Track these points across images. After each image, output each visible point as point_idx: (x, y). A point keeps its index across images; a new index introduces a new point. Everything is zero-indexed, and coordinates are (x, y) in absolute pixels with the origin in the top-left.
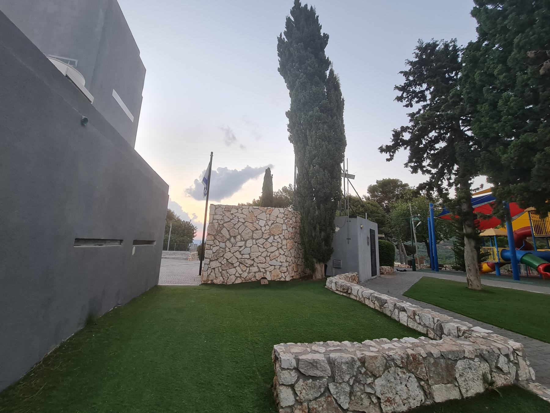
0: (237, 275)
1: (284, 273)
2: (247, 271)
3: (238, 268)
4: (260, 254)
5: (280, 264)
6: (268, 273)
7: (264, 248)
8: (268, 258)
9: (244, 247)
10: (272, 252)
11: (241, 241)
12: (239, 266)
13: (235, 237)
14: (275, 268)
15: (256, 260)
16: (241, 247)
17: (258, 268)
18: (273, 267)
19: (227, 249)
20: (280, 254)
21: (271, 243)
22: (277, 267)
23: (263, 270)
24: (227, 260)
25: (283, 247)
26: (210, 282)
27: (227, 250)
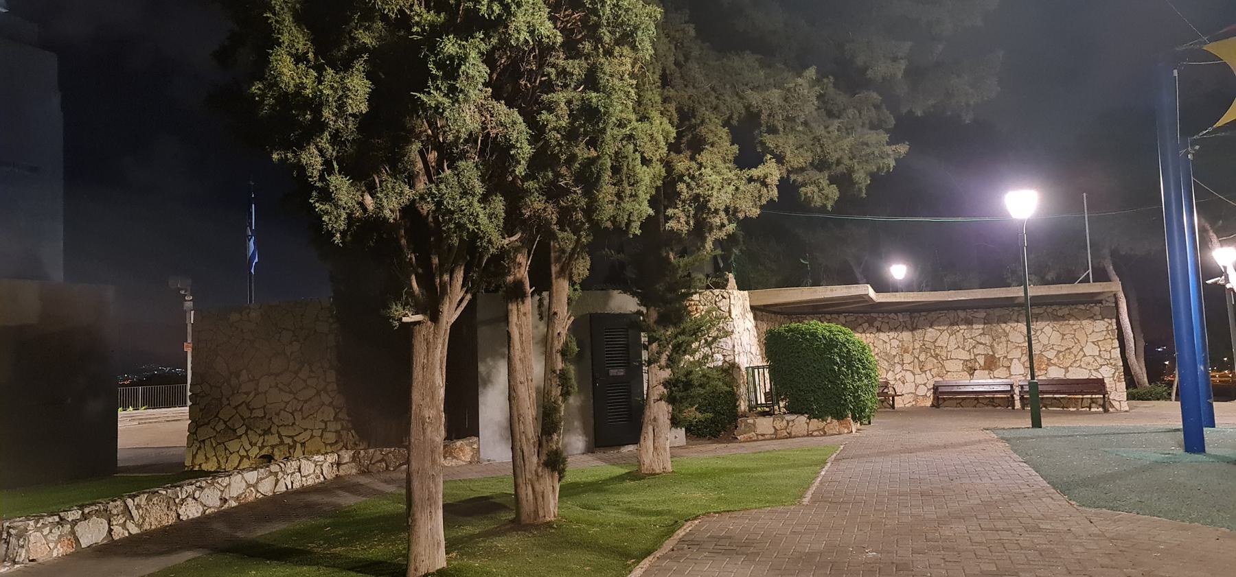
0: (243, 453)
1: (331, 445)
2: (259, 444)
3: (244, 438)
4: (283, 405)
5: (323, 426)
6: (298, 445)
7: (291, 392)
8: (298, 416)
9: (252, 395)
10: (305, 402)
11: (250, 380)
12: (246, 433)
13: (238, 376)
14: (312, 437)
15: (276, 420)
16: (248, 394)
17: (280, 436)
18: (309, 432)
19: (224, 399)
20: (323, 404)
21: (305, 381)
22: (317, 433)
23: (288, 441)
24: (225, 423)
25: (329, 388)
26: (197, 468)
27: (225, 402)
